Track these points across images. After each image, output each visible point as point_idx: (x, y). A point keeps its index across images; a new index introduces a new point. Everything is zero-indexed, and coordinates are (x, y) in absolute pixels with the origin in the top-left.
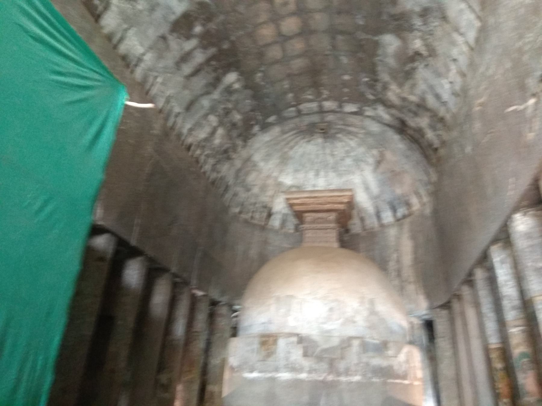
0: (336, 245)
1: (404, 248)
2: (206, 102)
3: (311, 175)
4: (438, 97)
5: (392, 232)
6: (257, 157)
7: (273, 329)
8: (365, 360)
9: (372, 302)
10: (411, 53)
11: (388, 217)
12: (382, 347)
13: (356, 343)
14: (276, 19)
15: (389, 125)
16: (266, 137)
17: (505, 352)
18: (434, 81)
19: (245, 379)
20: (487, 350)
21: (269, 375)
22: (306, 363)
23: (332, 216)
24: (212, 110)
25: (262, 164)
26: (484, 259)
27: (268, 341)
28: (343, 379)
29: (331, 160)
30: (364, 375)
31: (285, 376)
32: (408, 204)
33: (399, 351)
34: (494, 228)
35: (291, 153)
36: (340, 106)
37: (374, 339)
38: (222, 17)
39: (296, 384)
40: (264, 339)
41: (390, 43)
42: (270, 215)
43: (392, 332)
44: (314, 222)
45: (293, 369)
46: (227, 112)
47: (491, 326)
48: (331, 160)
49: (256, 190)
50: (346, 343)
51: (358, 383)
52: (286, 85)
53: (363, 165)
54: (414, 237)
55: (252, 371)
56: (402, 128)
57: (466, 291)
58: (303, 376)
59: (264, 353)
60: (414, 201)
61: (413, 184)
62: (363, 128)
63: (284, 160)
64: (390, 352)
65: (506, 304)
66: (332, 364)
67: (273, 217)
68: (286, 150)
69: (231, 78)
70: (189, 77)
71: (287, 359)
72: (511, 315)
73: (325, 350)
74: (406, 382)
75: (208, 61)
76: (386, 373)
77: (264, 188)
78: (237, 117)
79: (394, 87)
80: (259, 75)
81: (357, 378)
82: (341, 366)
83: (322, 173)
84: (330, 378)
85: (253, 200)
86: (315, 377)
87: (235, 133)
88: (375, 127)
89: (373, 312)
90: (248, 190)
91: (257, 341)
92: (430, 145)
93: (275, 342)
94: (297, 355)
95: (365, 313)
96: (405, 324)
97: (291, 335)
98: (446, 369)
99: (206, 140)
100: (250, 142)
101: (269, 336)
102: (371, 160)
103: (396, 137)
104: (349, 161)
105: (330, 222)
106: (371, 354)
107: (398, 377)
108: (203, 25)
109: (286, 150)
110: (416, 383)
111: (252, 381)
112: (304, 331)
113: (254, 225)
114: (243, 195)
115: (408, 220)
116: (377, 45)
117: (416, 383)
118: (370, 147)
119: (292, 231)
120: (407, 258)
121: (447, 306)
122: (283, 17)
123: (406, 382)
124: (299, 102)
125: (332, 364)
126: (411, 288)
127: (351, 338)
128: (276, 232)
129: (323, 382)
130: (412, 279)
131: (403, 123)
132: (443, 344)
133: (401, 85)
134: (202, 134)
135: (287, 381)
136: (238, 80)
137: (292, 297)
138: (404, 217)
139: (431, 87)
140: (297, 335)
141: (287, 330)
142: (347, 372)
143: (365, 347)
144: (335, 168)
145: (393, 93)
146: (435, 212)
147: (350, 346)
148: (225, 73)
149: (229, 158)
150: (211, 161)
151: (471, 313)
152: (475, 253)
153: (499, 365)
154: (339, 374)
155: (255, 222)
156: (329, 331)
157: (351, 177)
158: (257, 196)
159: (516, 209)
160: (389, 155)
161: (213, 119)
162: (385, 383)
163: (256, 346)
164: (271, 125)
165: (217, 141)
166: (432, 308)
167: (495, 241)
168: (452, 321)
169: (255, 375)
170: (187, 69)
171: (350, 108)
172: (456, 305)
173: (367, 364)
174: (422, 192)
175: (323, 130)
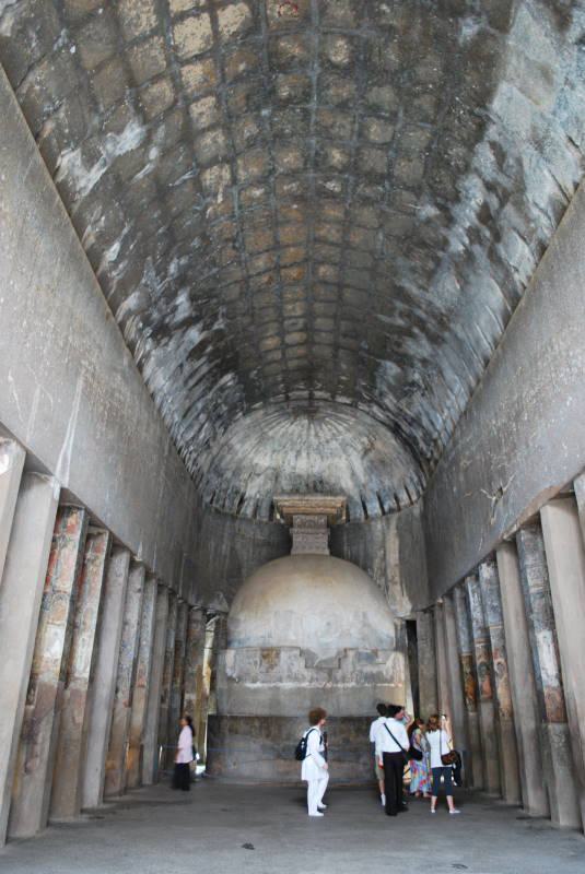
0: (327, 552)
1: (390, 546)
2: (200, 405)
3: (291, 455)
4: (432, 423)
5: (379, 526)
6: (234, 441)
7: (274, 642)
8: (358, 668)
9: (365, 615)
10: (410, 381)
11: (374, 508)
12: (372, 657)
13: (351, 654)
14: (282, 333)
15: (383, 423)
16: (248, 420)
17: (472, 659)
18: (431, 412)
19: (249, 689)
20: (460, 657)
21: (272, 685)
22: (308, 674)
23: (323, 520)
24: (203, 410)
25: (238, 447)
26: (461, 584)
27: (269, 654)
28: (340, 685)
29: (314, 441)
30: (357, 682)
31: (288, 685)
32: (396, 498)
33: (387, 658)
34: (470, 566)
35: (271, 433)
36: (333, 397)
37: (366, 648)
38: (232, 337)
39: (299, 691)
40: (265, 653)
41: (392, 369)
42: (242, 501)
43: (381, 641)
44: (302, 525)
45: (296, 679)
46: (216, 407)
47: (464, 638)
48: (314, 441)
49: (229, 474)
50: (342, 656)
51: (353, 688)
52: (279, 378)
53: (351, 450)
54: (400, 536)
55: (254, 682)
56: (396, 430)
57: (447, 602)
58: (305, 684)
59: (265, 665)
60: (404, 496)
61: (402, 477)
62: (354, 416)
63: (263, 439)
64: (380, 660)
65: (474, 624)
66: (330, 672)
67: (246, 503)
68: (266, 430)
69: (228, 379)
70: (190, 390)
71: (289, 670)
72: (477, 634)
73: (325, 661)
74: (393, 685)
75: (210, 371)
76: (375, 678)
77: (237, 473)
78: (225, 408)
79: (391, 397)
80: (255, 372)
81: (352, 684)
82: (339, 674)
83: (304, 454)
84: (329, 685)
85: (224, 486)
86: (315, 684)
87: (218, 424)
88: (368, 420)
89: (366, 625)
90: (220, 475)
91: (259, 653)
92: (422, 453)
93: (278, 655)
94: (299, 666)
95: (360, 626)
96: (392, 633)
97: (292, 648)
98: (425, 670)
99: (193, 438)
100: (230, 427)
101: (270, 649)
102: (360, 447)
103: (389, 434)
104: (334, 444)
105: (320, 526)
106: (364, 662)
107: (386, 681)
108: (214, 346)
109: (266, 430)
110: (400, 685)
111: (256, 691)
112: (305, 645)
113: (226, 515)
114: (215, 481)
115: (396, 515)
116: (379, 365)
117: (400, 685)
118: (360, 434)
119: (265, 520)
120: (393, 557)
121: (430, 610)
122: (289, 333)
123: (393, 685)
124: (287, 392)
125: (330, 672)
126: (396, 589)
127: (345, 650)
128: (250, 521)
129: (324, 689)
130: (397, 579)
131: (396, 424)
132: (423, 646)
133: (398, 399)
134: (191, 434)
135: (291, 689)
136: (234, 378)
137: (291, 612)
138: (391, 510)
139: (427, 414)
140: (297, 648)
141: (288, 644)
142: (344, 680)
143: (359, 656)
144: (319, 451)
145: (389, 401)
146: (424, 516)
147: (346, 656)
148: (222, 377)
149: (209, 447)
150: (194, 455)
151: (449, 622)
152: (456, 578)
153: (467, 670)
154: (337, 682)
155: (227, 511)
156: (327, 644)
157: (337, 460)
158: (228, 481)
159: (483, 561)
160: (378, 445)
161: (203, 417)
162: (375, 688)
163: (258, 660)
164: (255, 409)
165: (201, 436)
166: (413, 610)
167: (470, 574)
168: (433, 624)
169: (258, 685)
170: (191, 383)
171: (341, 399)
172: (438, 613)
173: (361, 672)
174: (412, 489)
175: (309, 411)
